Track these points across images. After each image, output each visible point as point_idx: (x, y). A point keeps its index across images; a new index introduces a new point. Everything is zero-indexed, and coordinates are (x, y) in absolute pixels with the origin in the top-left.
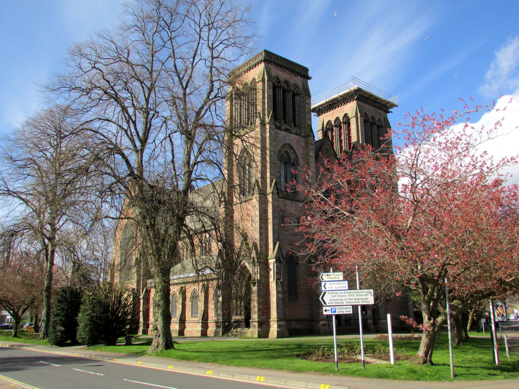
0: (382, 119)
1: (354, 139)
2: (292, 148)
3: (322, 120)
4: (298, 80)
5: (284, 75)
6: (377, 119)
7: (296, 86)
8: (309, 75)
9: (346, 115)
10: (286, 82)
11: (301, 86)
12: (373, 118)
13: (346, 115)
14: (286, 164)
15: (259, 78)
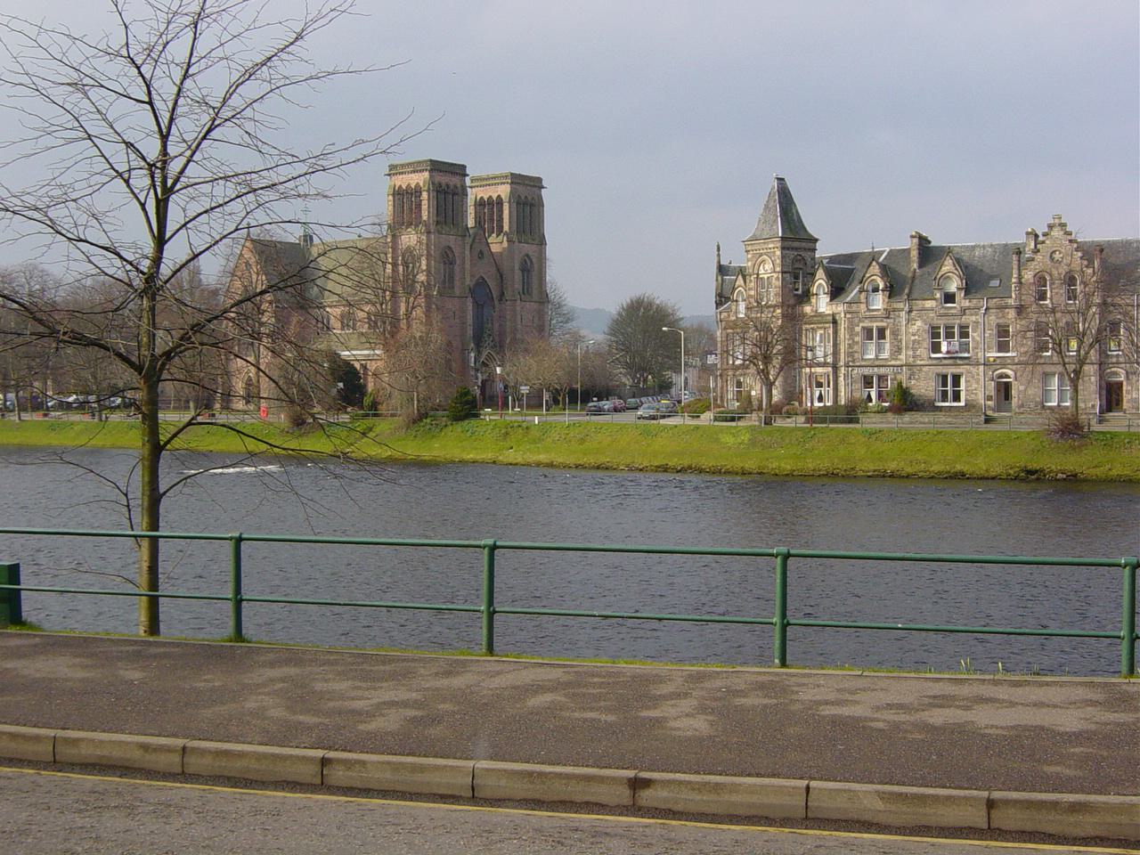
0: (536, 197)
1: (506, 228)
2: (450, 248)
3: (474, 193)
4: (455, 180)
5: (444, 179)
6: (529, 198)
7: (456, 187)
8: (468, 172)
9: (499, 196)
10: (448, 186)
11: (459, 186)
12: (526, 197)
13: (499, 196)
14: (445, 263)
15: (424, 186)
